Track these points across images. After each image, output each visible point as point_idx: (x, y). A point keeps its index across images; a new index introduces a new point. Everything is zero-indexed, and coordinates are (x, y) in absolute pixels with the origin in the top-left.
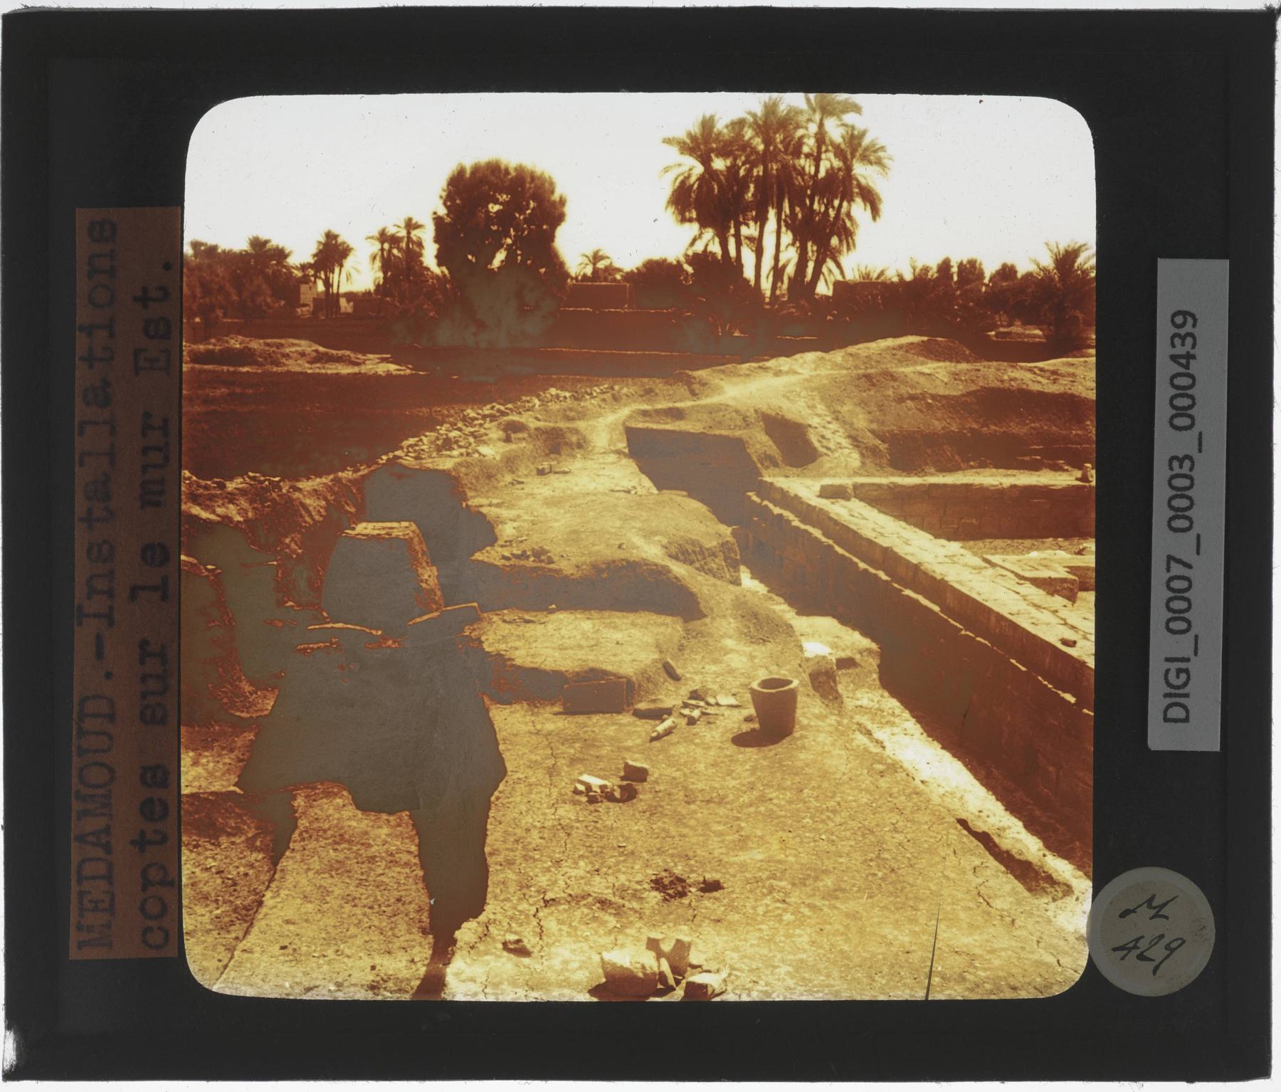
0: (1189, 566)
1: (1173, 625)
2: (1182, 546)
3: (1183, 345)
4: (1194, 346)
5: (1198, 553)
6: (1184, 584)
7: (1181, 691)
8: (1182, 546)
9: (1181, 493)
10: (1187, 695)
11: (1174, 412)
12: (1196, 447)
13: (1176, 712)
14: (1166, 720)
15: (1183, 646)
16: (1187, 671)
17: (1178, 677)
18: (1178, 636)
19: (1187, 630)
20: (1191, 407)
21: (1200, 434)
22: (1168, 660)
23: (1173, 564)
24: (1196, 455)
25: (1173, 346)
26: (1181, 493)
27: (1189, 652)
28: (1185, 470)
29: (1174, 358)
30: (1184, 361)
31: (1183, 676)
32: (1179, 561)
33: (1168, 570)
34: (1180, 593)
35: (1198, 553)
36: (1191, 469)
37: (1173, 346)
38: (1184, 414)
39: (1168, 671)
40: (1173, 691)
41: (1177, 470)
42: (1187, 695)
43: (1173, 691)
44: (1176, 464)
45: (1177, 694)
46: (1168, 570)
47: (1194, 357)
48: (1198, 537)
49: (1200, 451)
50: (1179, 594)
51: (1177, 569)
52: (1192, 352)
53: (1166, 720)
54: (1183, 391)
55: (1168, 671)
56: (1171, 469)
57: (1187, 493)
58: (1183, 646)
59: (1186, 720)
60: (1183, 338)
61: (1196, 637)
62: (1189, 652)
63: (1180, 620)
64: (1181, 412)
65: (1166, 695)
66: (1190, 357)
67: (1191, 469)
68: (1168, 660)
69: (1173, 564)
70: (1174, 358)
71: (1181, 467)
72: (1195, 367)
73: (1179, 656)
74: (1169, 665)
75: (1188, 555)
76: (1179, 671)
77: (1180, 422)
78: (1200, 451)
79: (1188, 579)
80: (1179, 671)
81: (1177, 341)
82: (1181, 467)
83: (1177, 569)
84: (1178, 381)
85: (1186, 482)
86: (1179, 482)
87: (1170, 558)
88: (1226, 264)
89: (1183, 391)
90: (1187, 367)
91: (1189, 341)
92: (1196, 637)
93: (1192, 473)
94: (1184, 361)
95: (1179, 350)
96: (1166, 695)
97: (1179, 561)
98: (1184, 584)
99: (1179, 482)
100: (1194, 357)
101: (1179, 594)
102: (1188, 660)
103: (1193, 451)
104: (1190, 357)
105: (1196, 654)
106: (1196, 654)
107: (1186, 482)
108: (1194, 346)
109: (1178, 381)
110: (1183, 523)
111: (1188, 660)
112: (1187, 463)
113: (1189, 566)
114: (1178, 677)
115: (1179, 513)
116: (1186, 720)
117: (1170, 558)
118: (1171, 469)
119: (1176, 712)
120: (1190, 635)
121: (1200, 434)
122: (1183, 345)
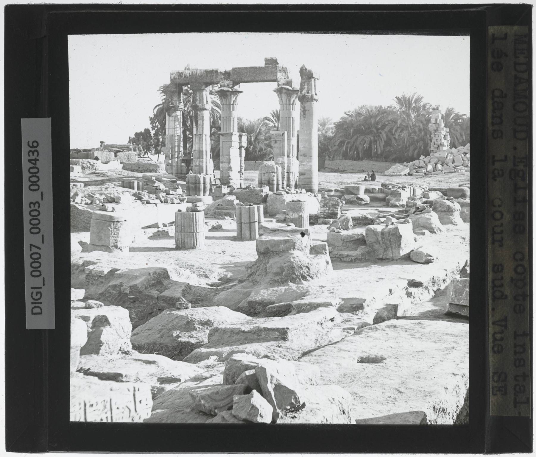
0: (40, 249)
1: (34, 274)
2: (36, 240)
3: (33, 155)
4: (38, 156)
5: (43, 243)
6: (38, 256)
7: (39, 301)
9: (35, 218)
10: (41, 303)
11: (31, 183)
13: (37, 310)
14: (33, 313)
16: (40, 293)
17: (37, 295)
19: (40, 275)
20: (38, 181)
21: (42, 192)
22: (32, 288)
23: (32, 247)
24: (40, 202)
25: (29, 155)
26: (35, 218)
27: (41, 285)
28: (36, 207)
29: (30, 161)
30: (34, 162)
33: (31, 250)
35: (43, 243)
36: (39, 207)
37: (29, 155)
39: (33, 292)
40: (35, 301)
41: (33, 208)
42: (41, 303)
43: (35, 301)
44: (32, 205)
45: (37, 303)
46: (31, 250)
47: (38, 160)
48: (43, 236)
49: (42, 199)
50: (35, 260)
51: (34, 250)
52: (37, 158)
53: (33, 313)
54: (34, 175)
55: (33, 292)
56: (30, 207)
57: (33, 269)
58: (38, 282)
59: (41, 313)
60: (33, 153)
62: (41, 285)
63: (37, 271)
64: (34, 183)
65: (32, 303)
66: (36, 160)
67: (39, 207)
68: (32, 288)
69: (32, 247)
70: (30, 161)
71: (34, 207)
72: (38, 164)
73: (37, 286)
74: (33, 290)
76: (37, 293)
77: (33, 188)
78: (42, 199)
79: (39, 254)
80: (37, 293)
81: (31, 154)
82: (34, 207)
83: (34, 250)
84: (32, 171)
85: (37, 213)
87: (31, 245)
89: (34, 175)
90: (35, 164)
91: (36, 153)
93: (39, 209)
95: (32, 157)
96: (32, 303)
98: (38, 256)
100: (38, 160)
101: (35, 260)
102: (41, 288)
103: (39, 200)
104: (36, 160)
105: (44, 285)
106: (44, 285)
107: (37, 213)
108: (38, 156)
109: (32, 171)
110: (36, 230)
111: (41, 288)
112: (37, 205)
113: (40, 249)
114: (37, 295)
115: (35, 226)
116: (41, 313)
117: (31, 245)
118: (30, 207)
119: (37, 310)
120: (41, 278)
121: (42, 192)
122: (33, 155)
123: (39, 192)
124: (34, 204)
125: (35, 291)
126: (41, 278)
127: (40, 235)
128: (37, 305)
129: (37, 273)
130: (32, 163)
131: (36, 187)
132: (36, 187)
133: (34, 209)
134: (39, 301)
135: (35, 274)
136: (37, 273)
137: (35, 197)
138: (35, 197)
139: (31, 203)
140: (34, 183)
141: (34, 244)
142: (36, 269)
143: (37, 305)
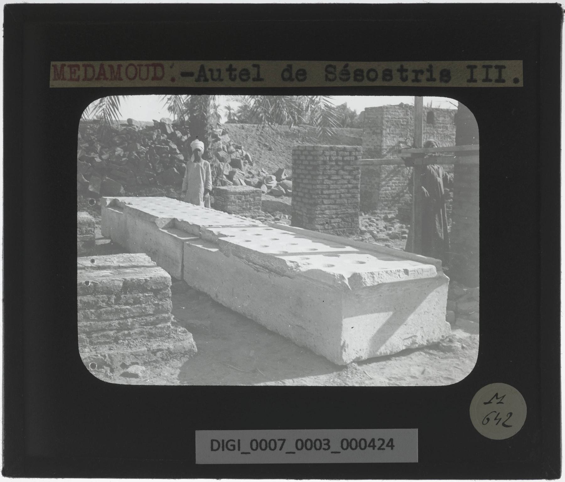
0: (281, 449)
2: (290, 446)
5: (287, 453)
7: (225, 449)
8: (290, 446)
10: (223, 450)
12: (335, 451)
13: (216, 445)
14: (212, 441)
15: (245, 447)
16: (234, 449)
17: (231, 445)
18: (249, 445)
20: (352, 449)
22: (239, 440)
23: (282, 442)
25: (379, 440)
26: (313, 445)
27: (242, 450)
28: (324, 446)
29: (373, 440)
30: (372, 444)
31: (232, 448)
32: (283, 445)
33: (279, 440)
34: (268, 445)
35: (287, 453)
36: (324, 449)
37: (379, 440)
38: (348, 444)
41: (323, 442)
42: (223, 450)
45: (224, 445)
46: (279, 440)
47: (374, 449)
49: (332, 452)
51: (279, 443)
52: (376, 448)
53: (212, 441)
56: (324, 440)
58: (245, 447)
59: (212, 450)
61: (249, 453)
62: (242, 450)
64: (349, 444)
65: (223, 441)
66: (374, 447)
67: (324, 449)
68: (239, 440)
69: (282, 442)
70: (373, 440)
71: (325, 444)
75: (286, 448)
76: (234, 446)
77: (345, 443)
78: (332, 452)
80: (234, 446)
82: (325, 444)
83: (279, 443)
84: (363, 442)
85: (318, 447)
86: (318, 443)
87: (284, 440)
88: (416, 460)
89: (358, 445)
90: (369, 446)
92: (249, 453)
93: (322, 450)
94: (372, 444)
96: (223, 441)
97: (283, 445)
99: (318, 443)
100: (374, 449)
101: (268, 445)
102: (239, 450)
103: (332, 449)
104: (374, 447)
105: (242, 453)
106: (242, 453)
107: (318, 447)
109: (363, 442)
110: (300, 445)
111: (239, 450)
112: (326, 447)
113: (281, 449)
114: (231, 445)
116: (212, 450)
117: (284, 440)
118: (324, 440)
119: (216, 445)
120: (250, 451)
123: (340, 450)
124: (328, 444)
125: (236, 444)
126: (249, 450)
127: (294, 450)
128: (221, 446)
129: (254, 446)
130: (370, 443)
131: (345, 446)
132: (345, 446)
133: (323, 445)
134: (225, 449)
135: (254, 444)
136: (254, 446)
137: (335, 446)
138: (335, 446)
139: (328, 441)
140: (349, 444)
141: (285, 444)
142: (259, 445)
143: (221, 446)
